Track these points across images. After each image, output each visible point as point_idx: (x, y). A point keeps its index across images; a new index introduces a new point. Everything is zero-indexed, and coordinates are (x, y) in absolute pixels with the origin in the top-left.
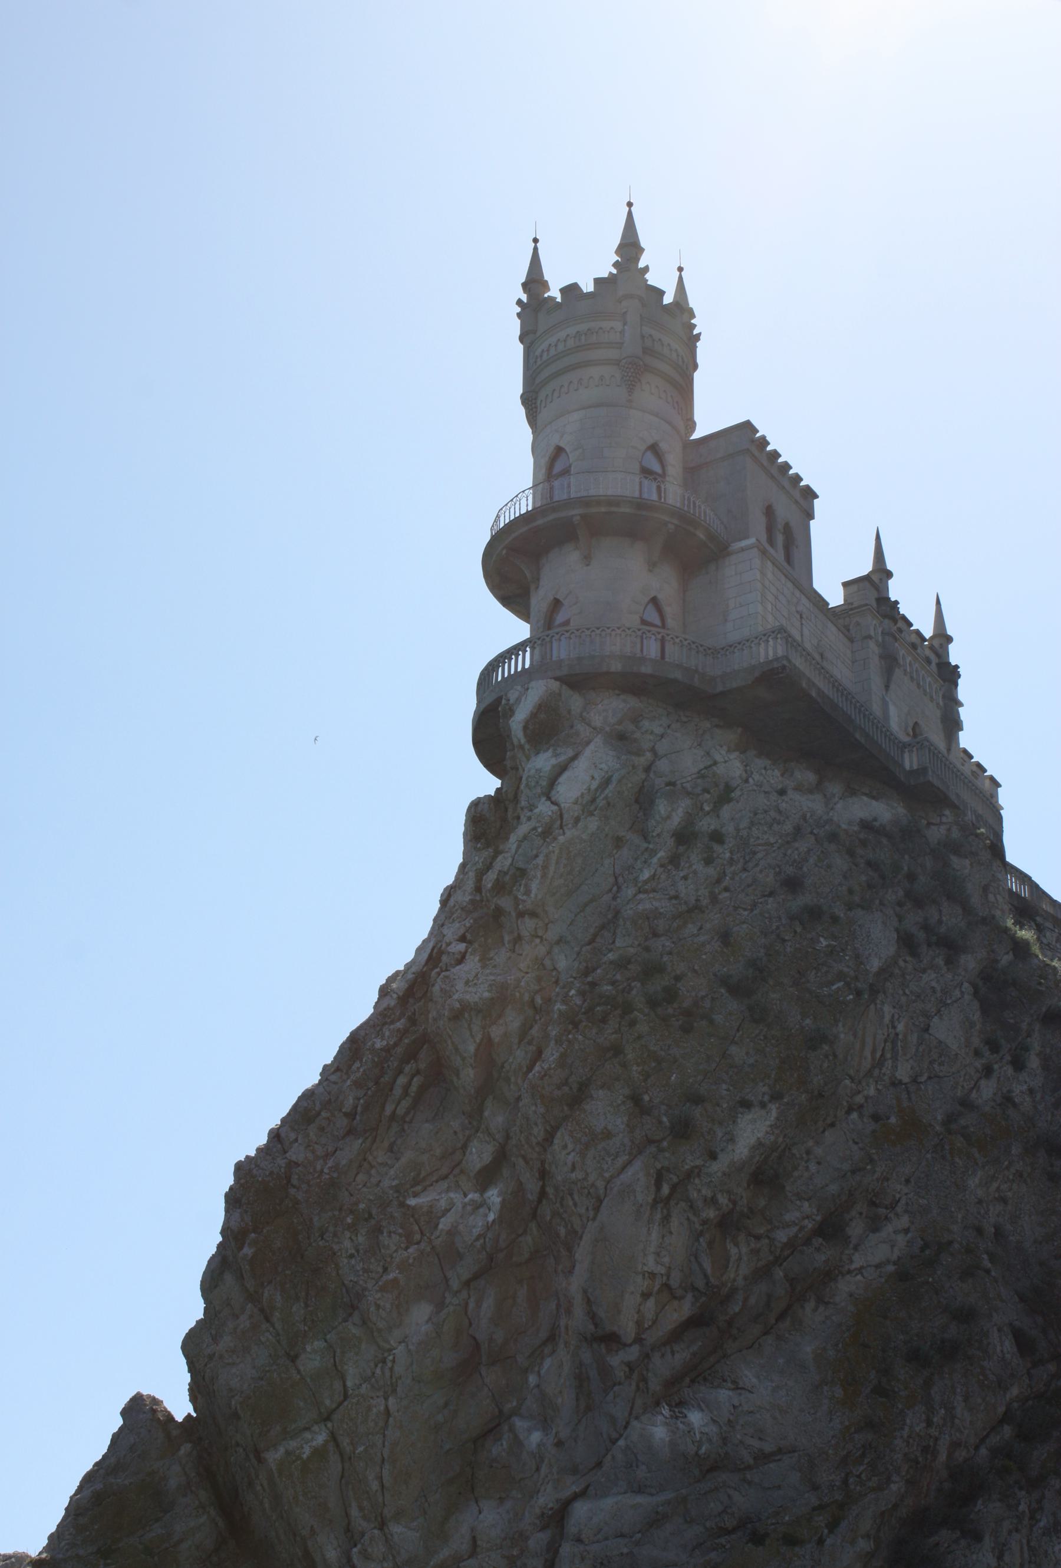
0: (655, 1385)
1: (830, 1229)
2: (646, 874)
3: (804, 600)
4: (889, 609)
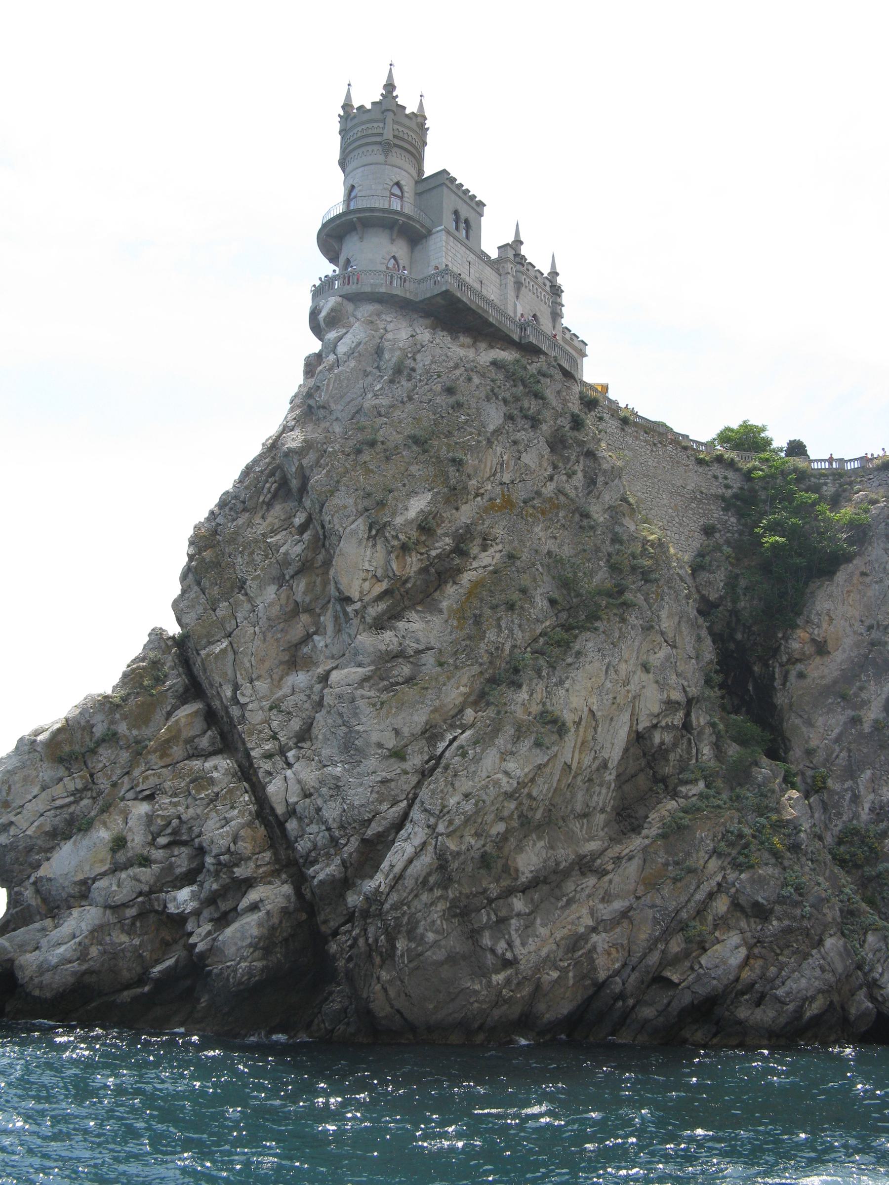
0: (369, 620)
1: (459, 550)
2: (378, 387)
3: (472, 255)
4: (520, 259)
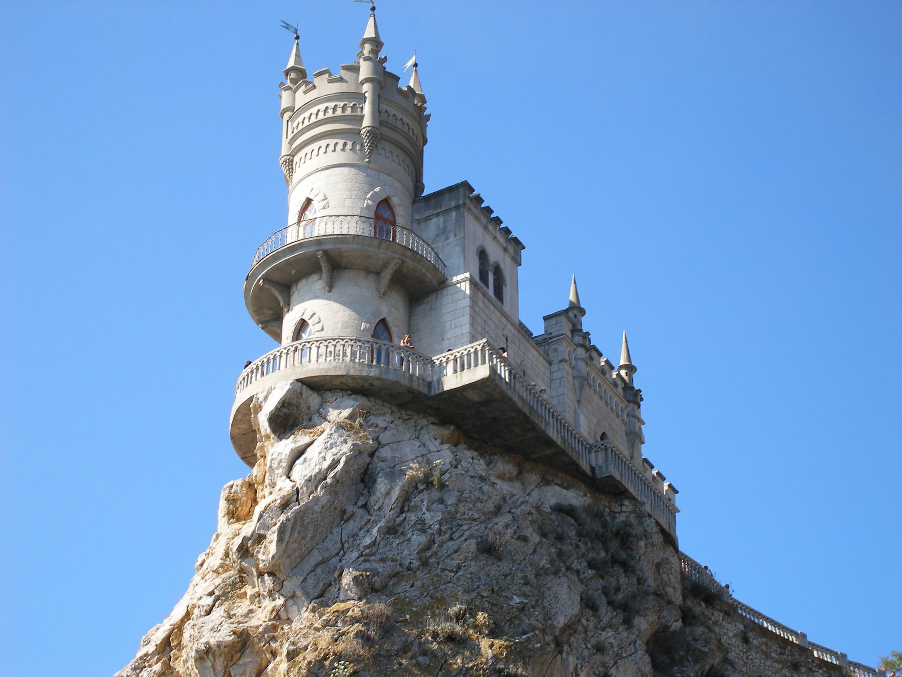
2: (368, 541)
3: (509, 327)
